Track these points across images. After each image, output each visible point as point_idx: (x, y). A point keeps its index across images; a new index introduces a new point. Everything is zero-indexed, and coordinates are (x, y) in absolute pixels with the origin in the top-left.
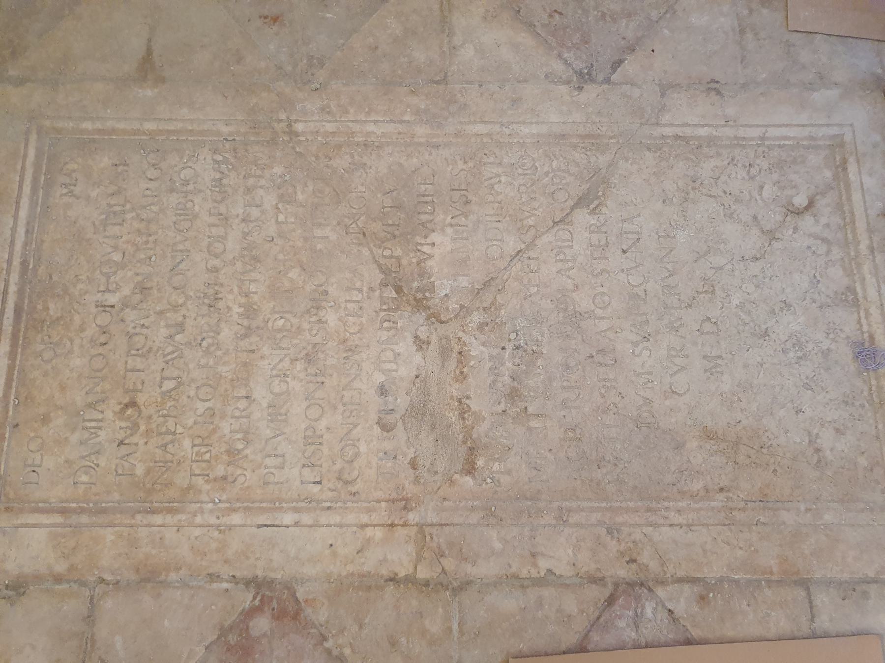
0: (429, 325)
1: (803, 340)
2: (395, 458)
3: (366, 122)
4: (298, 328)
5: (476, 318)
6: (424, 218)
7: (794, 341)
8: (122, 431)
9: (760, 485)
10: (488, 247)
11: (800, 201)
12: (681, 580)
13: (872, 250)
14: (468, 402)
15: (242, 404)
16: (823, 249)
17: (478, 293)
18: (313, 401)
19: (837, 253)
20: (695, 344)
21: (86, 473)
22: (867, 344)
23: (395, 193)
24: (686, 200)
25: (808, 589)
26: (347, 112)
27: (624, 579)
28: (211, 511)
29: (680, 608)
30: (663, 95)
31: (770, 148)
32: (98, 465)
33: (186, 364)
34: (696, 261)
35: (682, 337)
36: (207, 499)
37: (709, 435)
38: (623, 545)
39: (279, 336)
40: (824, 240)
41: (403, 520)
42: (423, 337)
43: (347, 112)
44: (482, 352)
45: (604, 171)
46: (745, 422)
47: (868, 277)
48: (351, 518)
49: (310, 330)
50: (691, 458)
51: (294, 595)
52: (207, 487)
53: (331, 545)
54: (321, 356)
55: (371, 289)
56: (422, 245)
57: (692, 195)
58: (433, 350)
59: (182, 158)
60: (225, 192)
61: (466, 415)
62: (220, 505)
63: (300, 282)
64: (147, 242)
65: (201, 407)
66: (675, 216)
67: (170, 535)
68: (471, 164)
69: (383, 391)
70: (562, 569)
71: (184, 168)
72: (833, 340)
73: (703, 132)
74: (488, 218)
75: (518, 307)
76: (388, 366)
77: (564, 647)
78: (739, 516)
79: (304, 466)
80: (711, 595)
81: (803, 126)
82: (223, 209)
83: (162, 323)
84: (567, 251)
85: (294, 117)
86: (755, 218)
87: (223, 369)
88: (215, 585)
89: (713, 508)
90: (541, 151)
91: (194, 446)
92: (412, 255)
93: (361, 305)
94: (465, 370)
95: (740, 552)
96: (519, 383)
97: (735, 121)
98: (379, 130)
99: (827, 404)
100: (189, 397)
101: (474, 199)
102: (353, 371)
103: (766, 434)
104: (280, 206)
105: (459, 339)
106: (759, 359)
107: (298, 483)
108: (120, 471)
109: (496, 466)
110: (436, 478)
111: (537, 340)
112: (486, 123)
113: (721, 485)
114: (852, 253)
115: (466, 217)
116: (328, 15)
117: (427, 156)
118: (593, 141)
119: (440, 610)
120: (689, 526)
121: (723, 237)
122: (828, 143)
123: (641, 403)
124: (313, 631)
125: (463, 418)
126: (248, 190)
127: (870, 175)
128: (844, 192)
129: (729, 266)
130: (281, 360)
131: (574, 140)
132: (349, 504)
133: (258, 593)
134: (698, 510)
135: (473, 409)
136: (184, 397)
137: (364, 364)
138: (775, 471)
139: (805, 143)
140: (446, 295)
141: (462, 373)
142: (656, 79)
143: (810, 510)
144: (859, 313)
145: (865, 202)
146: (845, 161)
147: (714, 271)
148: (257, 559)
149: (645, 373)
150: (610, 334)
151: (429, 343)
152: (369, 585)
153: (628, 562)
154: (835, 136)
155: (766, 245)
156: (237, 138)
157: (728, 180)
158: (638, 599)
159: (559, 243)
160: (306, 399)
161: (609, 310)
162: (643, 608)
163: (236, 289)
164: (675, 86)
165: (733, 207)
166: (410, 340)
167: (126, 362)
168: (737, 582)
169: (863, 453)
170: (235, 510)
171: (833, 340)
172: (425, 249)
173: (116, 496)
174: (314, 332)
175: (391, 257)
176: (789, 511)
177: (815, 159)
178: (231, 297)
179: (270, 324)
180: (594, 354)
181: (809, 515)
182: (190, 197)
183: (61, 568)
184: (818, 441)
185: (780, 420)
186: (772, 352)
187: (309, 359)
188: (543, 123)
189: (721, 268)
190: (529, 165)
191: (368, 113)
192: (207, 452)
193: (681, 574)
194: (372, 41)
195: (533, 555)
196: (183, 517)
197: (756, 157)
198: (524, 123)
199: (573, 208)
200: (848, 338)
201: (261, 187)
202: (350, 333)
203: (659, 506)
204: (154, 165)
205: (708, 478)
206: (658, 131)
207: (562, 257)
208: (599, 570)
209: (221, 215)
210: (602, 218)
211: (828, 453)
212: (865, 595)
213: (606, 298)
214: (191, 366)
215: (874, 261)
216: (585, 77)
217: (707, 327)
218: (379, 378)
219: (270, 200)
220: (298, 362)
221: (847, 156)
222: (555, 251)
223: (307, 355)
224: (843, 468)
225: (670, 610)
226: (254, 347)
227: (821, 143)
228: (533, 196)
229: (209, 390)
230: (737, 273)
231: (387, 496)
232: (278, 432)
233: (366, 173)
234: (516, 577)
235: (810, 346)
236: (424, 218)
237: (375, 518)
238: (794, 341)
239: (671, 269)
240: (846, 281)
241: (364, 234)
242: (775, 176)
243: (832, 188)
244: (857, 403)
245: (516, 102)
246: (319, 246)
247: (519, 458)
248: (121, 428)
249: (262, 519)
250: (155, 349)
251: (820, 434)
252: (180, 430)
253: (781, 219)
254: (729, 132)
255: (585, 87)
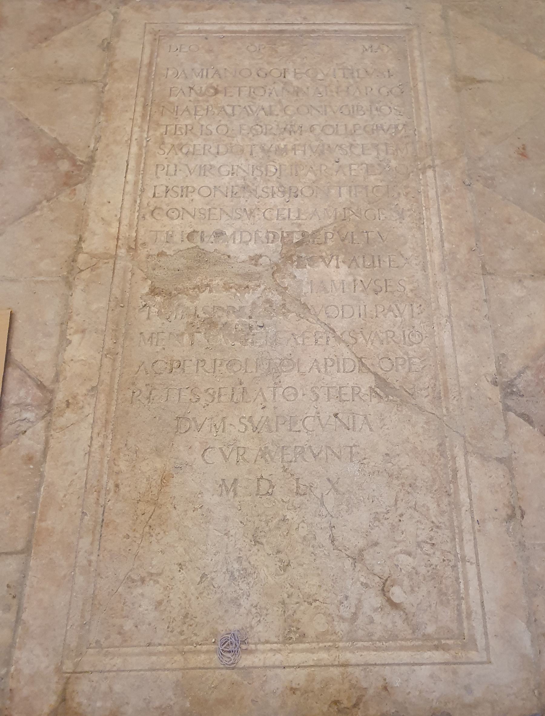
0: (270, 265)
1: (250, 579)
2: (167, 242)
3: (440, 216)
4: (269, 180)
5: (277, 298)
6: (360, 261)
7: (249, 570)
8: (199, 88)
9: (118, 521)
10: (337, 307)
11: (397, 594)
12: (47, 442)
13: (345, 665)
14: (207, 291)
15: (214, 150)
16: (347, 615)
17: (297, 300)
18: (213, 191)
19: (342, 627)
20: (250, 472)
21: (173, 74)
22: (244, 647)
23: (380, 240)
24: (390, 476)
25: (22, 552)
26: (446, 203)
27: (55, 398)
28: (141, 136)
29: (25, 440)
30: (500, 460)
31: (454, 567)
32: (178, 78)
33: (243, 118)
34: (329, 480)
35: (255, 461)
36: (150, 134)
37: (165, 479)
38: (82, 398)
39: (263, 169)
40: (355, 616)
41: (121, 246)
42: (261, 261)
43: (446, 203)
44: (247, 302)
45: (413, 402)
46: (174, 513)
47: (315, 657)
48: (126, 213)
49: (267, 188)
50: (147, 462)
51: (80, 182)
52: (158, 134)
53: (109, 202)
54: (247, 195)
55: (300, 225)
56: (337, 259)
57: (395, 482)
58: (250, 268)
59: (398, 106)
60: (373, 133)
61: (197, 290)
62: (145, 141)
63: (304, 180)
64: (332, 91)
65: (213, 128)
66: (373, 464)
67: (129, 115)
68: (410, 294)
69: (219, 234)
70: (70, 352)
71: (390, 108)
72: (250, 612)
73: (463, 496)
74: (362, 307)
75: (285, 328)
76: (238, 237)
77: (13, 350)
78: (92, 498)
79: (167, 187)
80: (31, 467)
81: (483, 606)
82: (358, 132)
83: (272, 104)
84: (335, 367)
85: (437, 169)
86: (376, 544)
87: (239, 138)
88: (93, 141)
89: (102, 476)
90: (428, 349)
91: (186, 126)
92: (328, 252)
93: (287, 219)
94: (233, 290)
95: (61, 495)
96: (221, 329)
97: (479, 531)
98: (434, 226)
99: (186, 597)
100: (220, 121)
101: (379, 297)
102: (235, 214)
103: (162, 532)
104: (364, 166)
105: (259, 286)
106: (232, 532)
107: (155, 184)
108: (173, 89)
109: (154, 310)
110: (150, 268)
111: (256, 342)
112: (449, 304)
113: (121, 486)
114: (341, 644)
115: (362, 291)
116: (534, 190)
117: (414, 262)
118: (442, 393)
119: (54, 269)
120: (89, 453)
121: (354, 510)
122: (466, 632)
123: (199, 422)
124: (55, 193)
125: (194, 288)
126: (376, 146)
127: (432, 676)
128: (409, 644)
129: (325, 513)
130: (244, 171)
131: (441, 377)
132: (137, 214)
133: (84, 163)
134: (101, 462)
135: (200, 294)
136: (220, 118)
137: (240, 221)
138: (128, 536)
139: (464, 606)
140: (295, 277)
141: (231, 288)
142: (517, 455)
143: (90, 565)
144: (276, 643)
145: (399, 665)
146: (445, 648)
147: (320, 497)
148: (106, 162)
149: (224, 424)
150: (260, 399)
151: (256, 265)
152: (80, 226)
153: (67, 401)
154: (473, 640)
155: (347, 553)
156: (417, 137)
157: (414, 520)
158: (39, 407)
159: (341, 362)
160: (215, 187)
161: (282, 400)
162: (32, 411)
163: (297, 142)
164: (511, 473)
165: (386, 522)
166: (258, 252)
167: (245, 87)
168: (38, 490)
169: (136, 627)
170: (140, 149)
171: (250, 612)
172: (334, 263)
173: (157, 89)
174: (265, 190)
175: (326, 238)
176: (92, 544)
177: (446, 615)
178: (292, 140)
179: (272, 163)
180: (243, 386)
181: (85, 562)
182: (367, 113)
183: (116, 66)
184: (151, 582)
185: (174, 547)
186: (238, 546)
187: (245, 188)
188: (454, 350)
189: (322, 504)
190: (413, 339)
191: (447, 218)
192: (181, 132)
193: (52, 442)
194: (516, 220)
195: (83, 331)
196: (139, 121)
197: (443, 552)
198: (452, 334)
199: (375, 374)
200: (252, 627)
201: (378, 154)
202: (264, 213)
203: (110, 431)
204: (391, 91)
205: (127, 475)
206: (459, 452)
207: (330, 363)
208: (65, 378)
209: (355, 131)
210: (366, 398)
211: (140, 591)
212: (7, 608)
213: (292, 398)
214: (242, 121)
215: (333, 666)
216: (509, 389)
217: (264, 485)
218: (229, 232)
219: (369, 159)
220: (243, 180)
221: (452, 652)
222: (335, 358)
223: (248, 186)
224: (124, 603)
225: (25, 432)
226: (254, 155)
227: (465, 624)
228: (385, 342)
229: (225, 132)
230: (318, 519)
231: (140, 238)
232: (192, 171)
233: (396, 220)
234: (70, 318)
235: (244, 586)
236: (360, 261)
237: (124, 228)
238: (249, 570)
239: (320, 456)
240: (311, 633)
241: (343, 220)
242: (423, 570)
243: (414, 632)
244: (185, 628)
245: (473, 328)
246: (333, 191)
247: (160, 325)
248: (201, 88)
249: (132, 164)
250: (254, 101)
251: (157, 585)
252: (197, 117)
253: (375, 572)
254: (467, 524)
255: (498, 387)
